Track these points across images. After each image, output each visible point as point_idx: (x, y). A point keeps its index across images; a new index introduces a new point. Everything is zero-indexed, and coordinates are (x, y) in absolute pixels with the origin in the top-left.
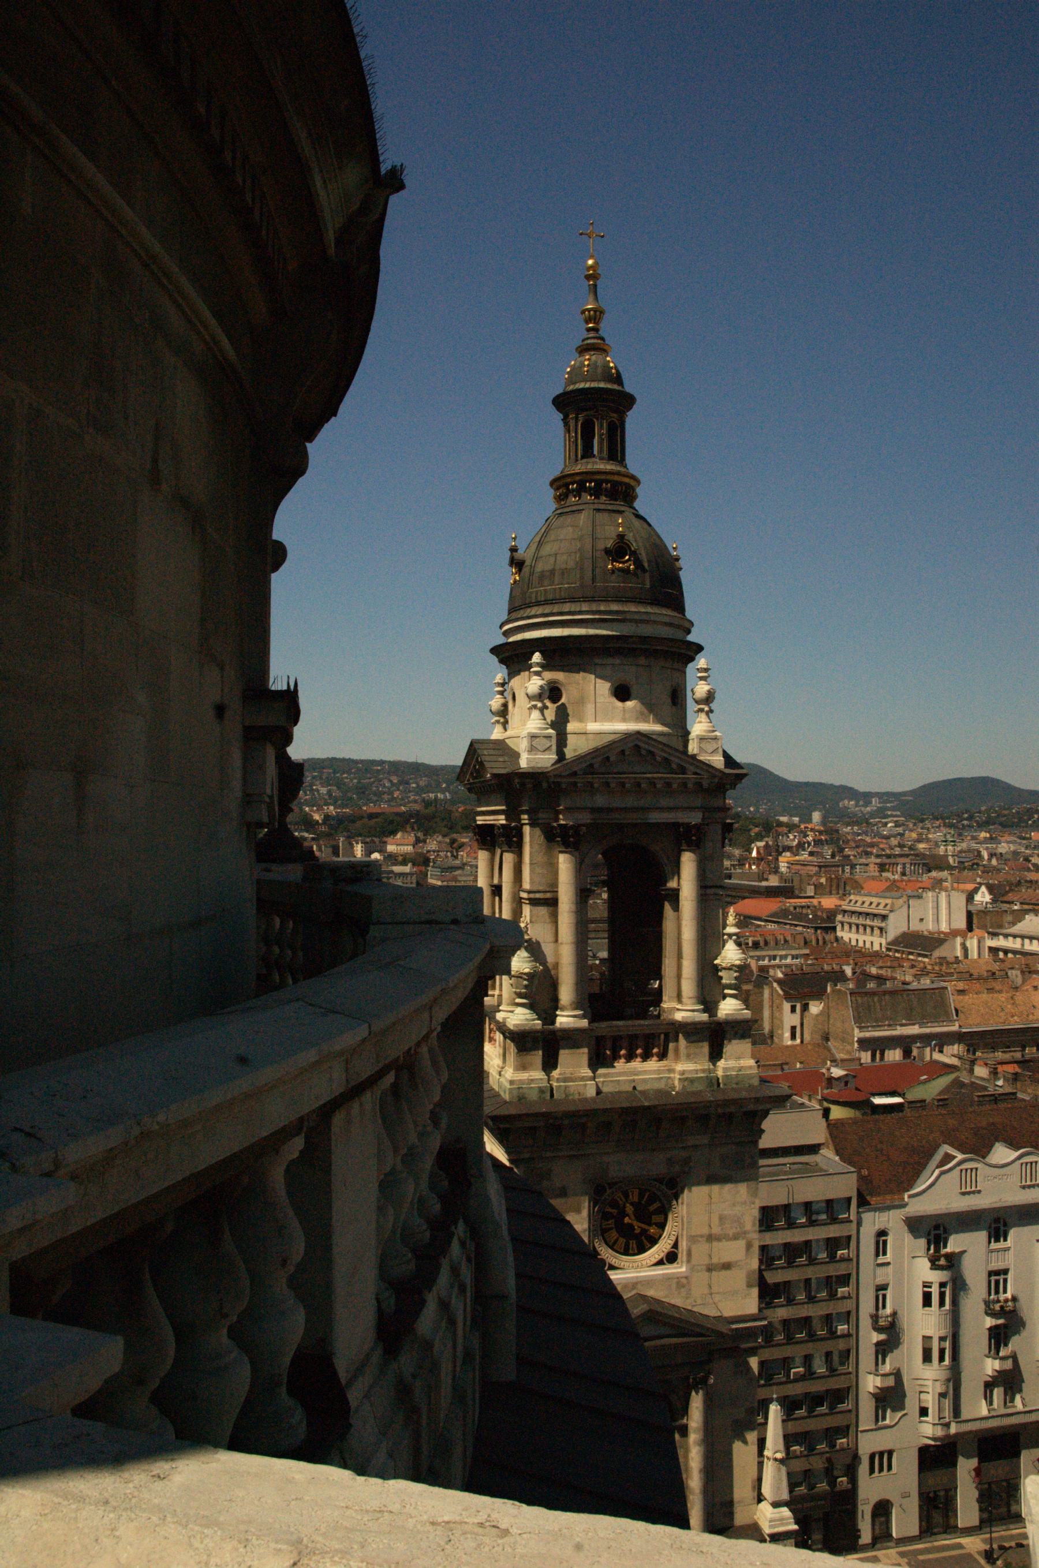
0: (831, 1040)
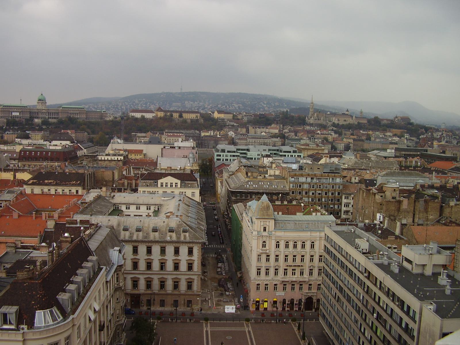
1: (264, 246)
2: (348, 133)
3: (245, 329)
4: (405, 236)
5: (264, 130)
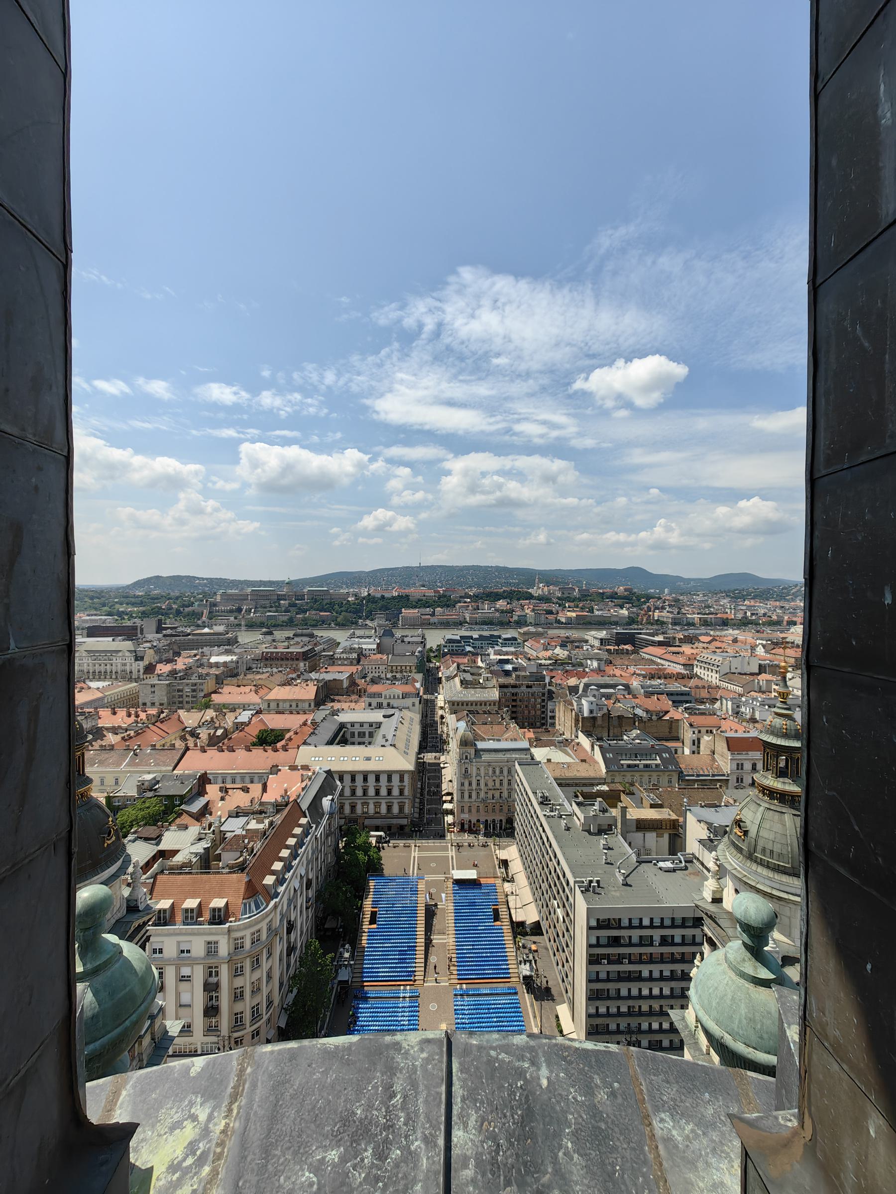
1: (466, 771)
2: (572, 604)
5: (493, 605)
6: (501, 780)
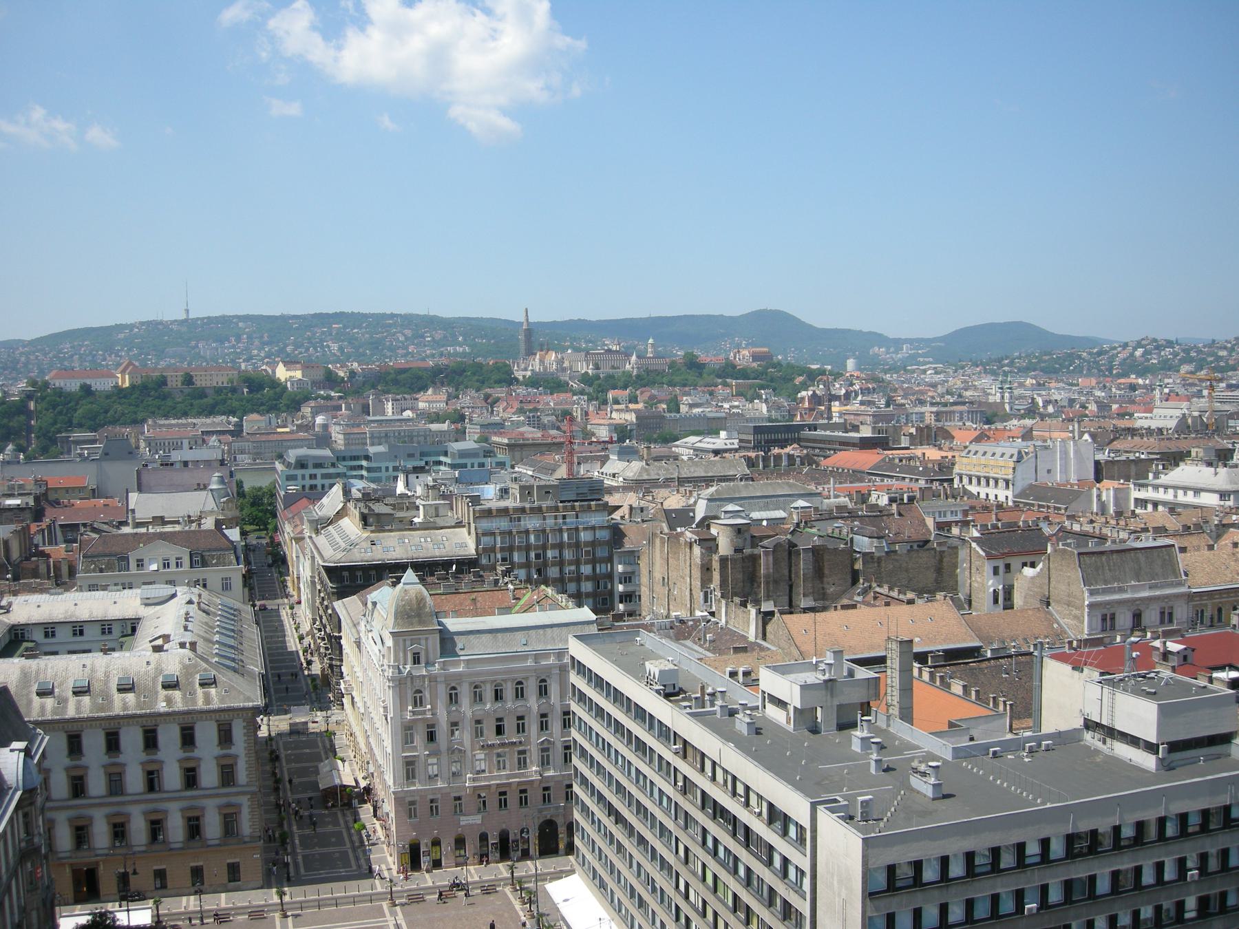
0: (1052, 604)
1: (418, 702)
2: (624, 394)
3: (387, 921)
4: (772, 643)
5: (409, 403)
6: (520, 718)
